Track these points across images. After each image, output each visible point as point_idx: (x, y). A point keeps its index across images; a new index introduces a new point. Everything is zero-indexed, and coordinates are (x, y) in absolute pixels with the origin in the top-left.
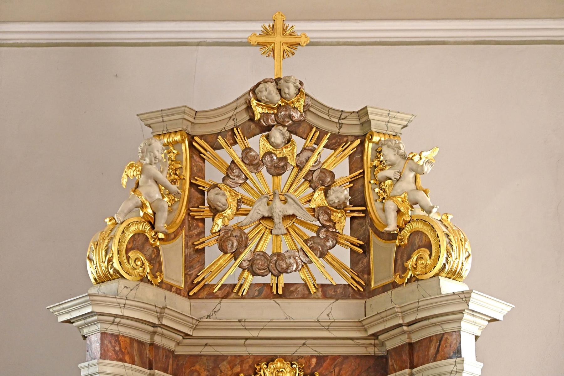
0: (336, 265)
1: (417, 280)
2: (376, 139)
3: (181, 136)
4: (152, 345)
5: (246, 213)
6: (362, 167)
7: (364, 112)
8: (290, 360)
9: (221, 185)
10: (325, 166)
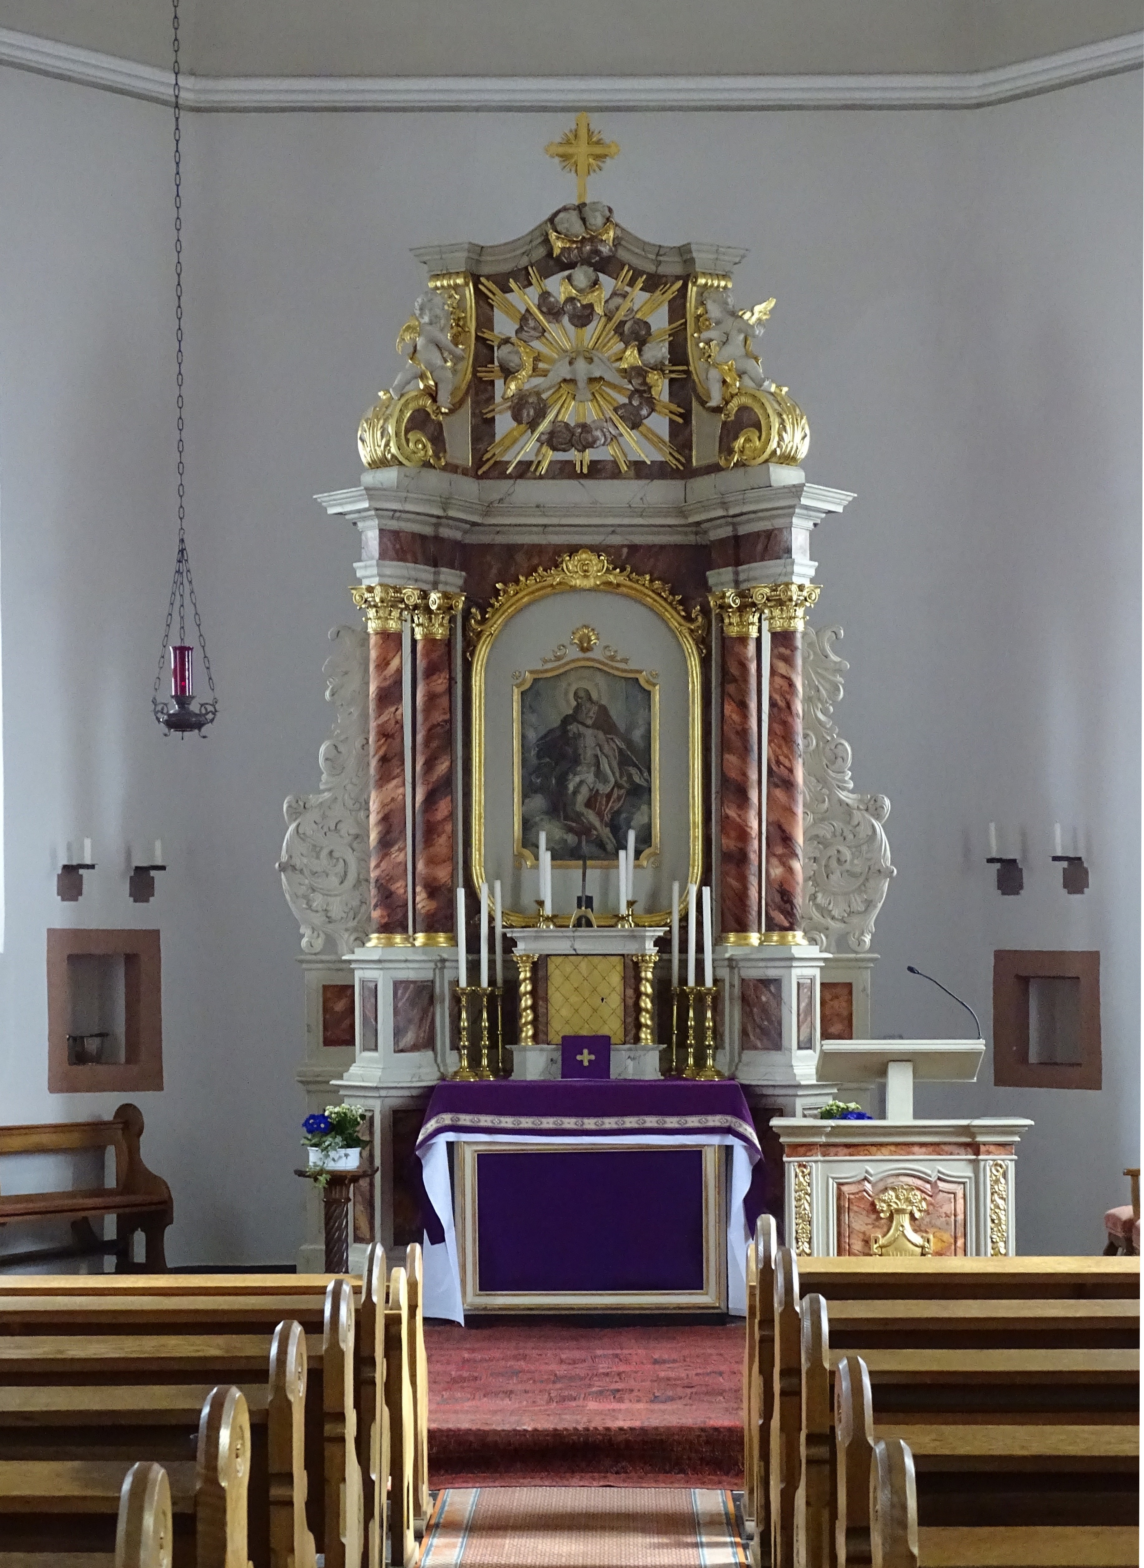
0: (651, 437)
1: (744, 465)
2: (702, 281)
3: (465, 278)
4: (437, 538)
5: (545, 374)
6: (684, 316)
8: (596, 550)
9: (514, 339)
10: (638, 316)
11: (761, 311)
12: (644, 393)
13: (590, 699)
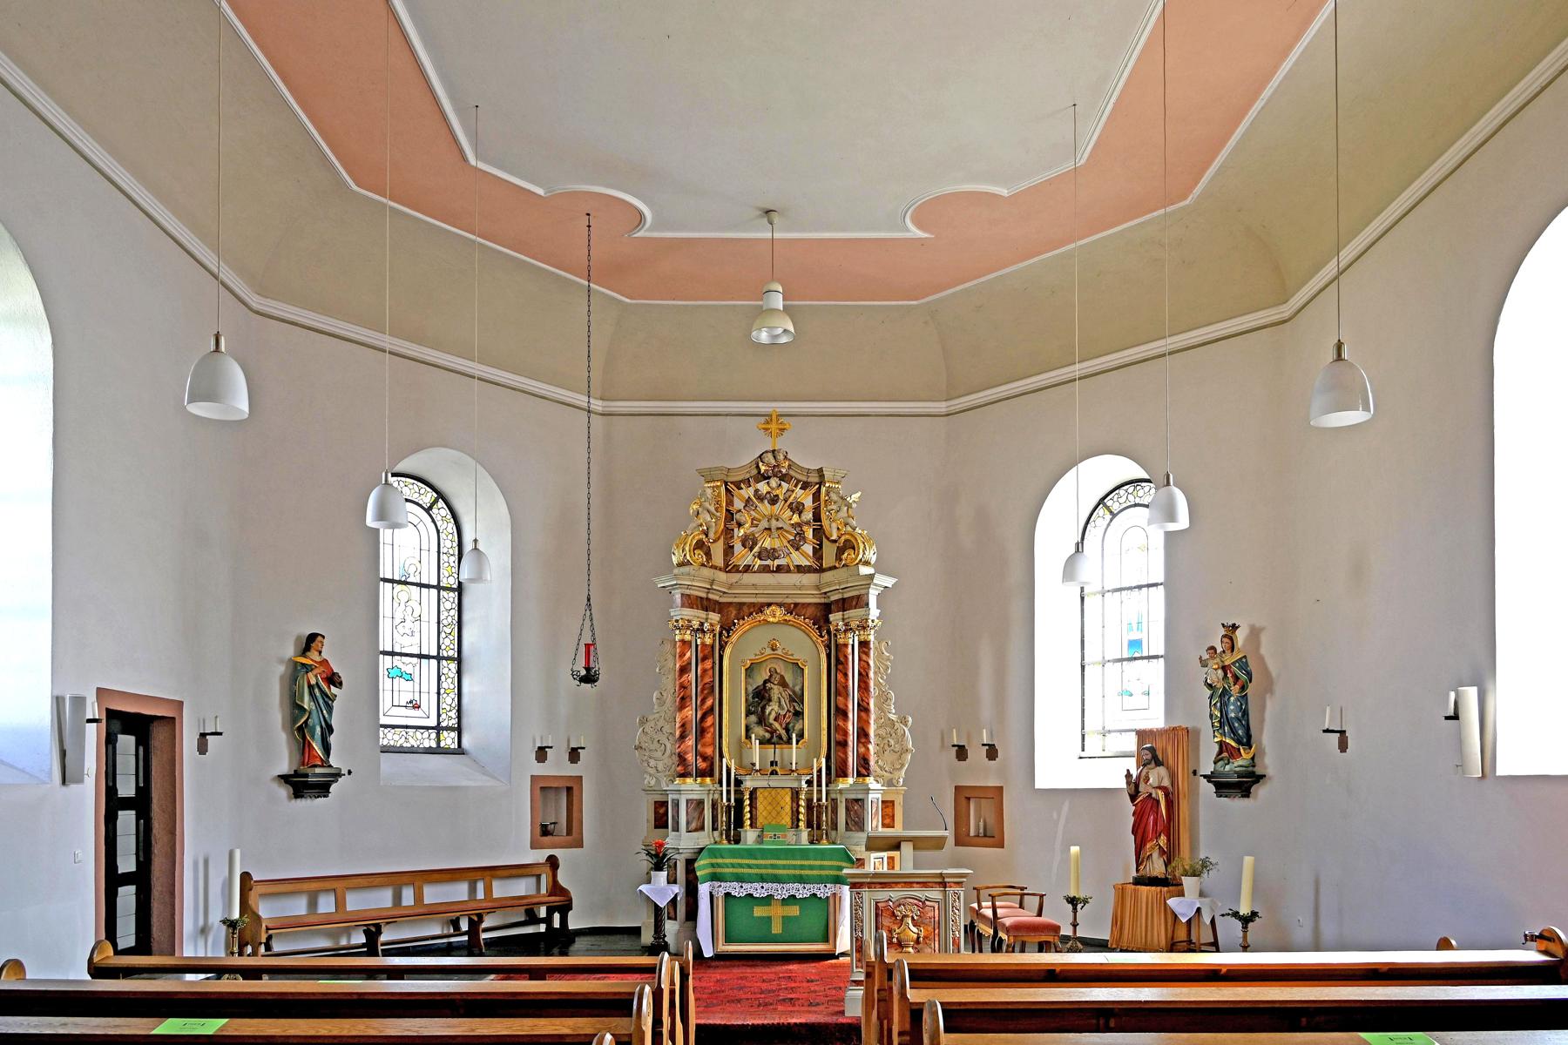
0: (804, 555)
2: (827, 485)
4: (707, 598)
7: (820, 471)
8: (780, 605)
11: (855, 497)
12: (801, 535)
13: (776, 672)
